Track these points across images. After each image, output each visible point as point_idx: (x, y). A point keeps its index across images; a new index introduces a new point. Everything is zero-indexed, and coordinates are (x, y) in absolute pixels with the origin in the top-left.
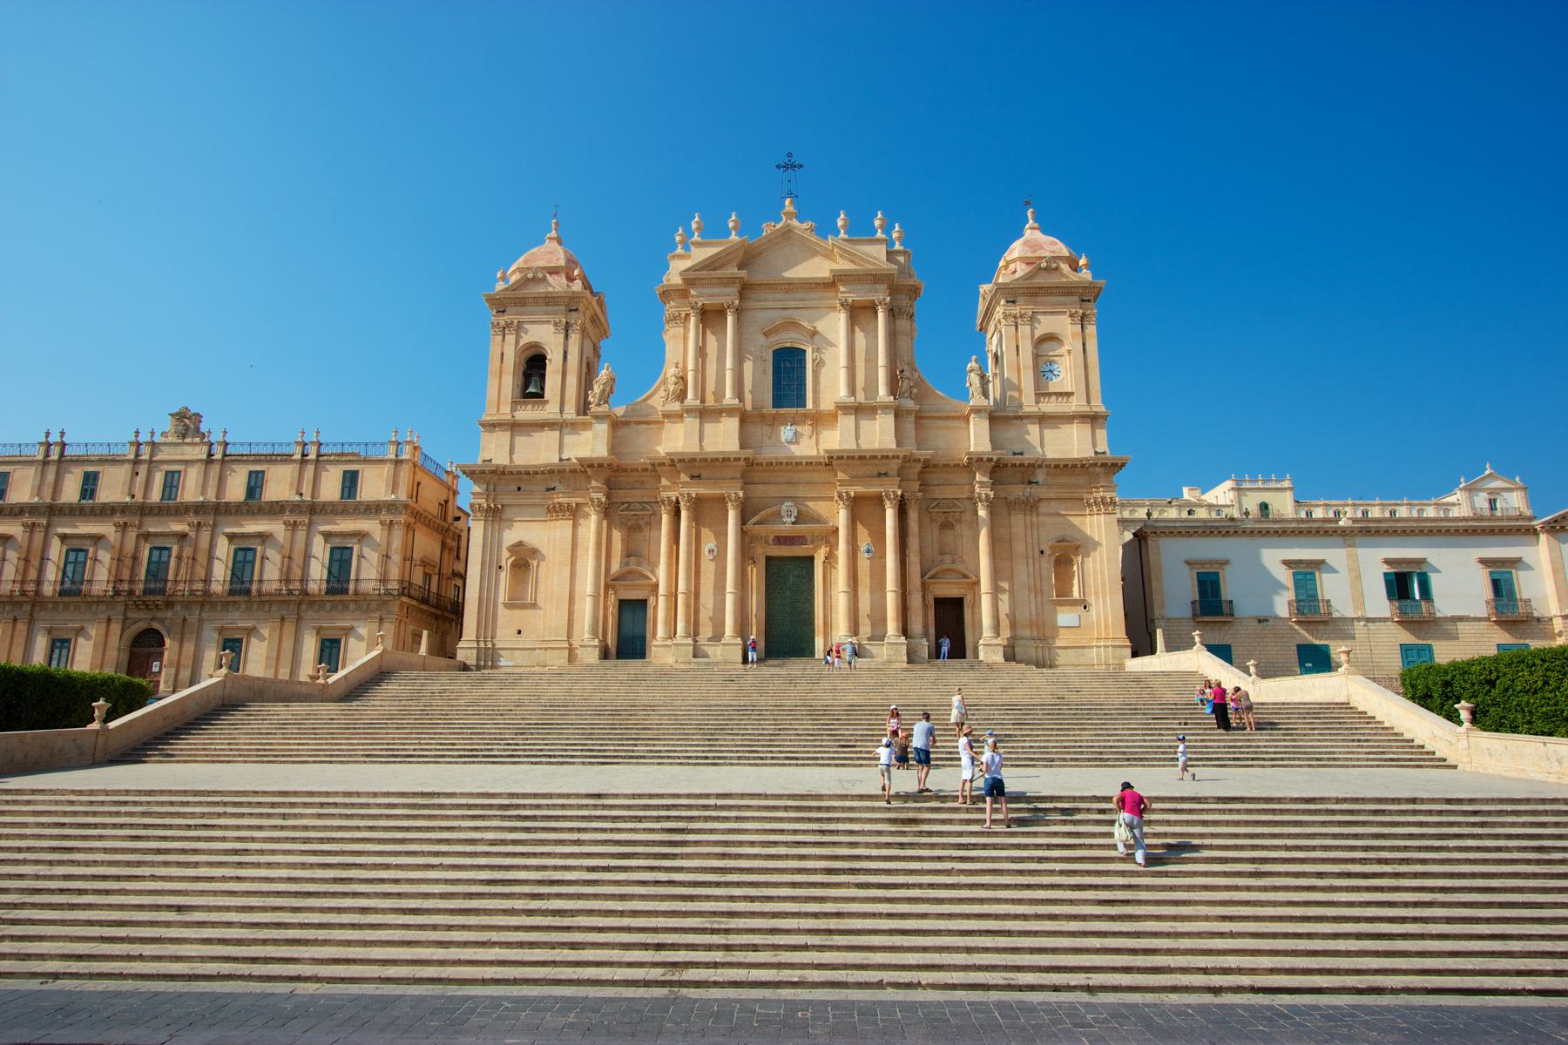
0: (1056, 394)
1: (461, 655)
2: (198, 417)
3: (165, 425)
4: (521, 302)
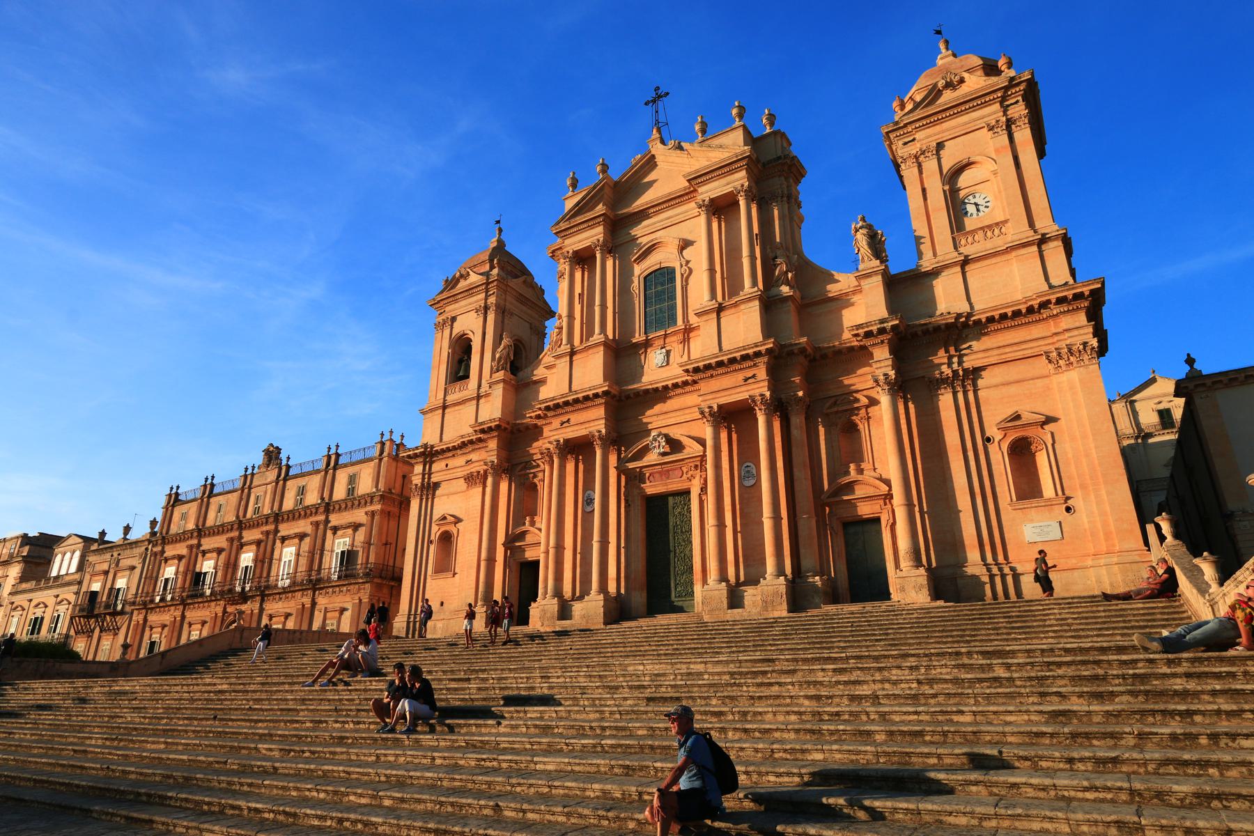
0: (982, 228)
1: (395, 633)
2: (278, 450)
3: (259, 459)
4: (454, 299)
